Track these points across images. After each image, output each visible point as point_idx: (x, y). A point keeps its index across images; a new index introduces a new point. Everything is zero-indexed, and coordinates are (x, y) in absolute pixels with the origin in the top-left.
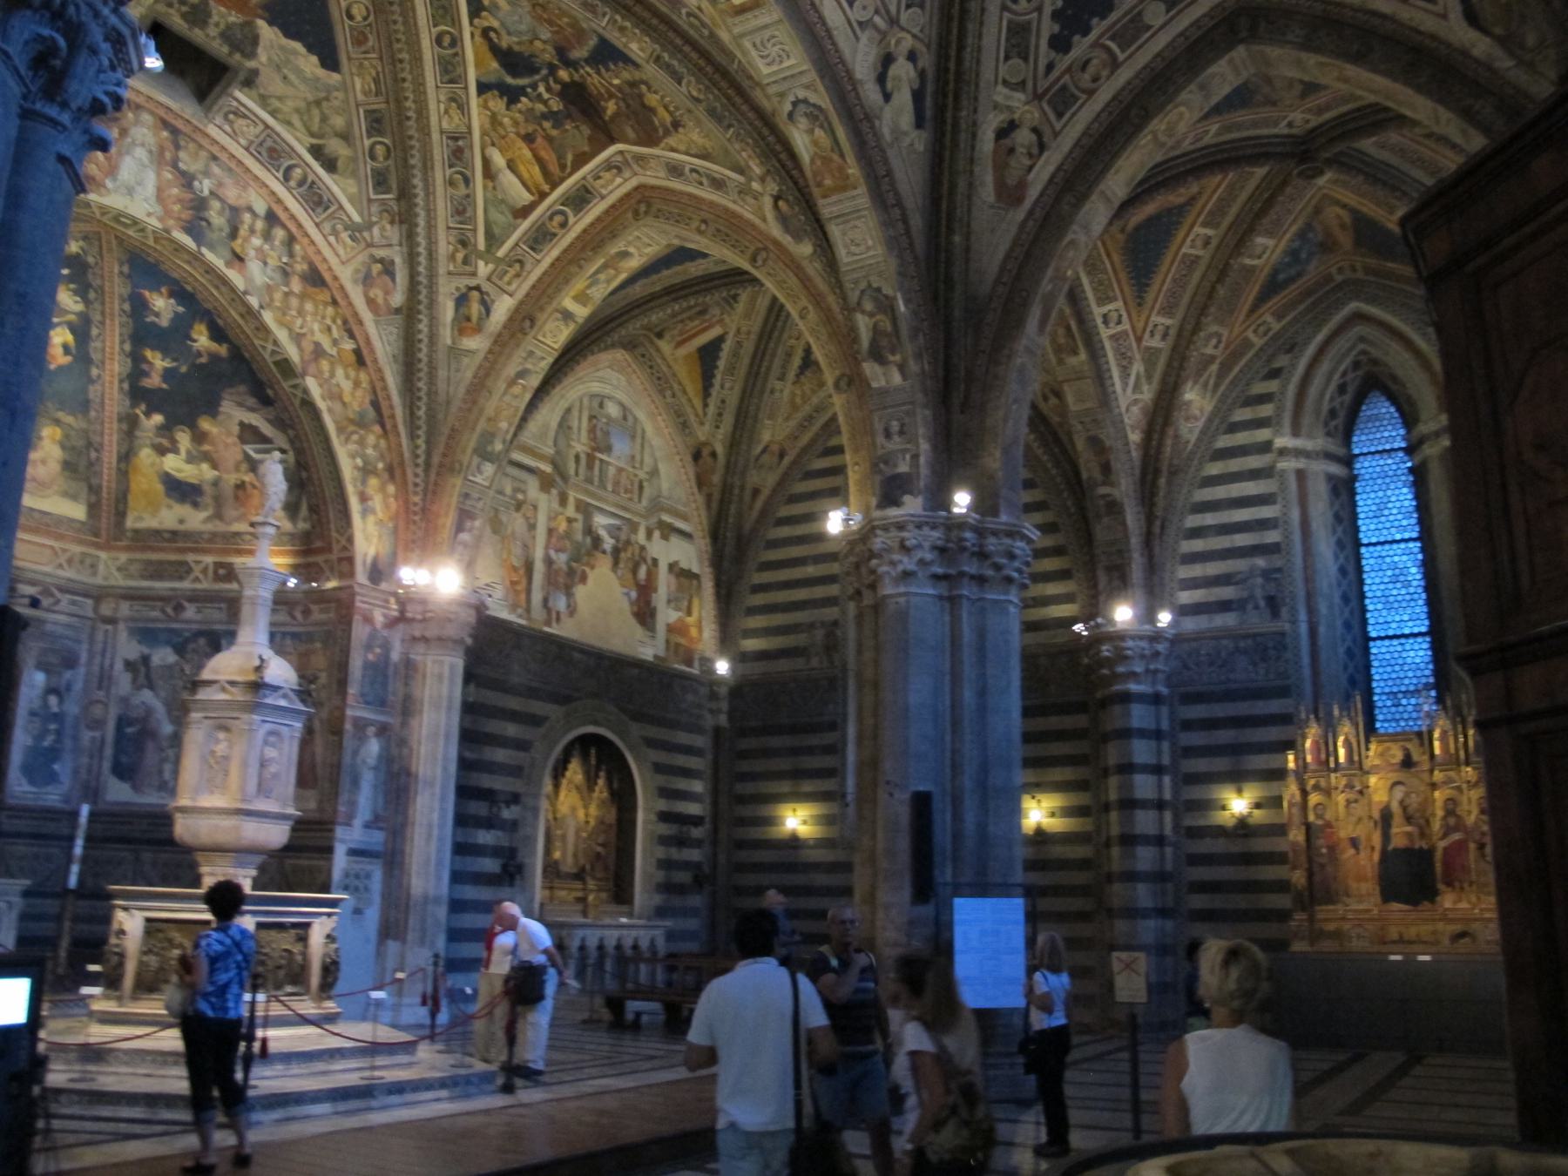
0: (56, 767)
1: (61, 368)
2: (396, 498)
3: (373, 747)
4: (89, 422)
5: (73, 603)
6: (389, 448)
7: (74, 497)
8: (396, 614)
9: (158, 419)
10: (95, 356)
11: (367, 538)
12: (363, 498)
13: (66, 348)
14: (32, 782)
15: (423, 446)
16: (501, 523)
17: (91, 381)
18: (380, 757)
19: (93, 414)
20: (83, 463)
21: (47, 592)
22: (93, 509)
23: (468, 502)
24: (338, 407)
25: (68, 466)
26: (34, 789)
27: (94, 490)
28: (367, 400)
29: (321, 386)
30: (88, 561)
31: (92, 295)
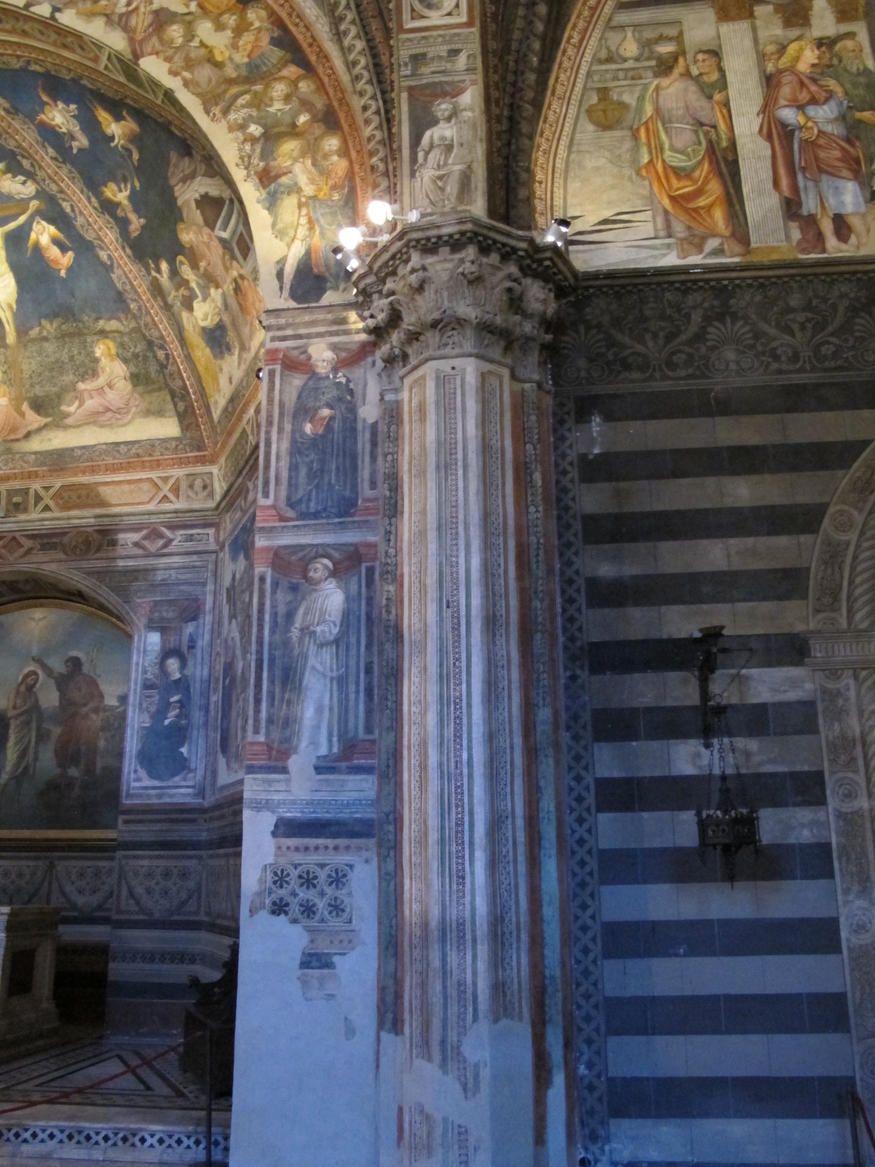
0: (184, 750)
1: (70, 270)
2: (344, 152)
3: (331, 598)
4: (134, 317)
5: (190, 538)
6: (321, 87)
7: (160, 413)
8: (363, 337)
9: (164, 266)
10: (89, 236)
11: (280, 234)
12: (266, 177)
13: (55, 241)
14: (152, 775)
15: (360, 45)
16: (624, 106)
17: (109, 269)
18: (347, 614)
19: (133, 306)
20: (153, 368)
21: (154, 534)
22: (186, 417)
23: (425, 70)
24: (205, 73)
25: (136, 379)
26: (157, 783)
27: (179, 395)
28: (265, 40)
29: (168, 59)
30: (198, 483)
31: (26, 163)
